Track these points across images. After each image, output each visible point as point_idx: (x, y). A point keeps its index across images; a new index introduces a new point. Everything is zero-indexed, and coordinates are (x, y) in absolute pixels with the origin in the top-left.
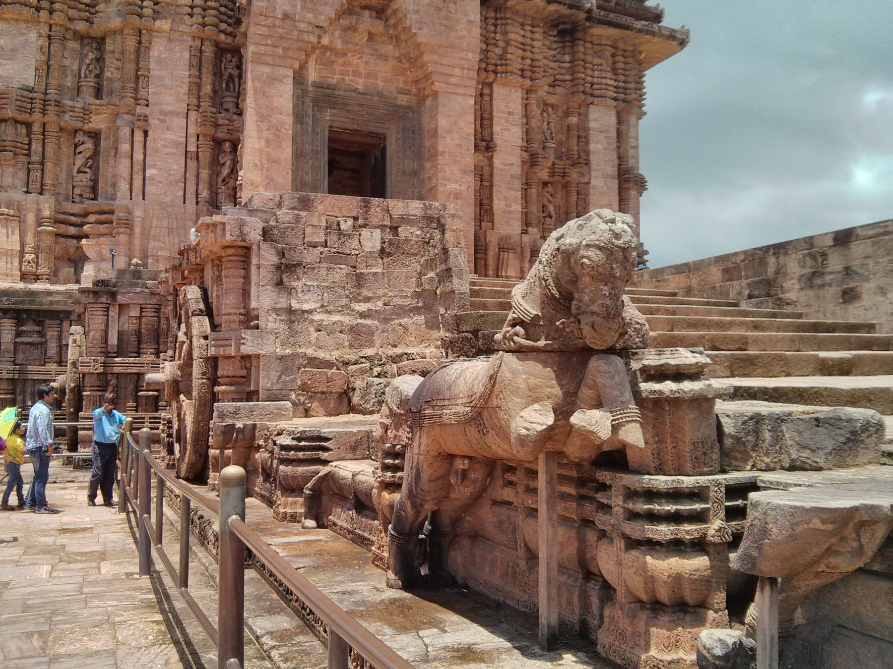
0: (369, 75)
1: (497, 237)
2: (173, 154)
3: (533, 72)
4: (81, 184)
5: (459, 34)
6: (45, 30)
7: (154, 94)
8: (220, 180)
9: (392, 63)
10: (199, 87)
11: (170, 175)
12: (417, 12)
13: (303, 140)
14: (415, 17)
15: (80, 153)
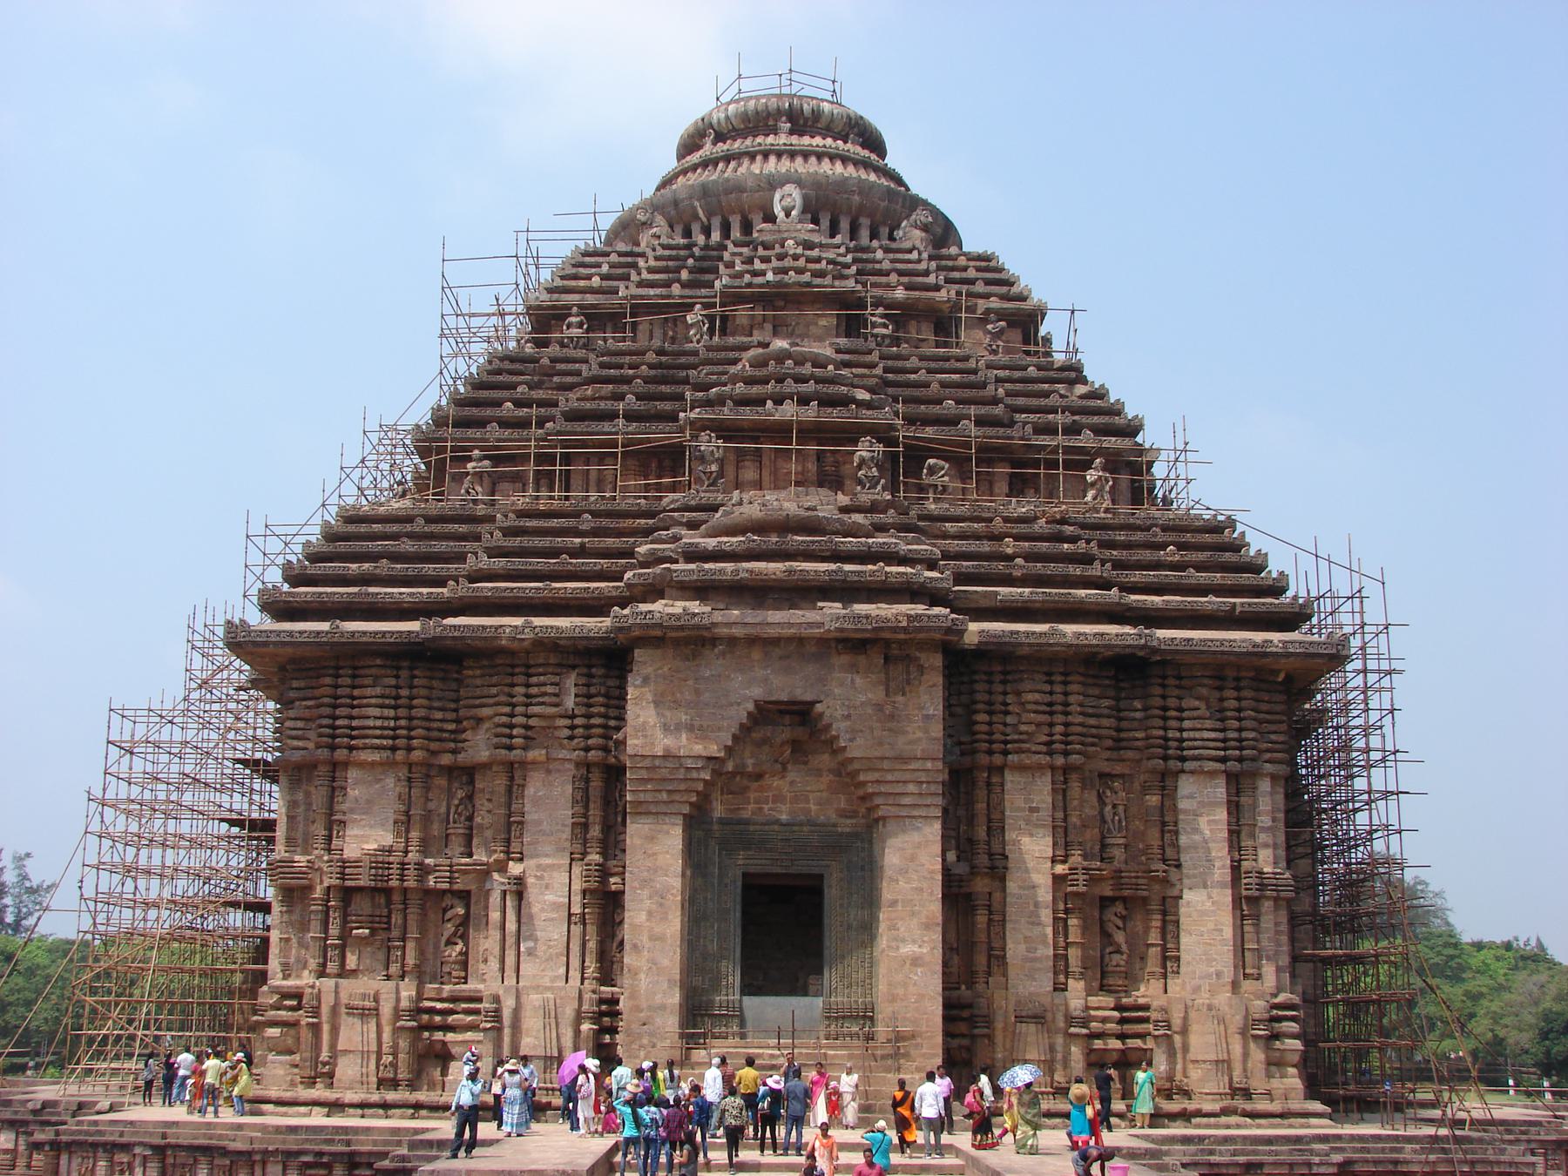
0: (795, 800)
1: (1012, 1000)
2: (552, 919)
3: (1067, 743)
4: (451, 959)
5: (911, 737)
6: (403, 773)
7: (529, 844)
8: (615, 945)
9: (827, 778)
10: (585, 827)
11: (550, 947)
12: (848, 717)
13: (706, 898)
14: (844, 725)
15: (449, 920)
